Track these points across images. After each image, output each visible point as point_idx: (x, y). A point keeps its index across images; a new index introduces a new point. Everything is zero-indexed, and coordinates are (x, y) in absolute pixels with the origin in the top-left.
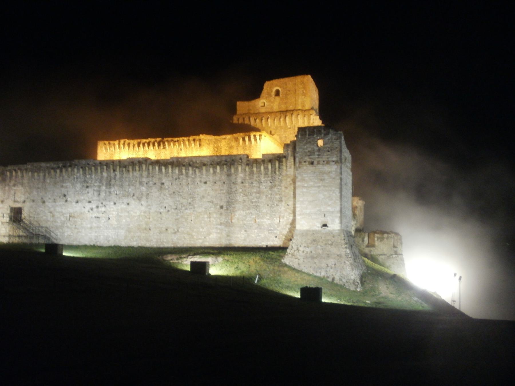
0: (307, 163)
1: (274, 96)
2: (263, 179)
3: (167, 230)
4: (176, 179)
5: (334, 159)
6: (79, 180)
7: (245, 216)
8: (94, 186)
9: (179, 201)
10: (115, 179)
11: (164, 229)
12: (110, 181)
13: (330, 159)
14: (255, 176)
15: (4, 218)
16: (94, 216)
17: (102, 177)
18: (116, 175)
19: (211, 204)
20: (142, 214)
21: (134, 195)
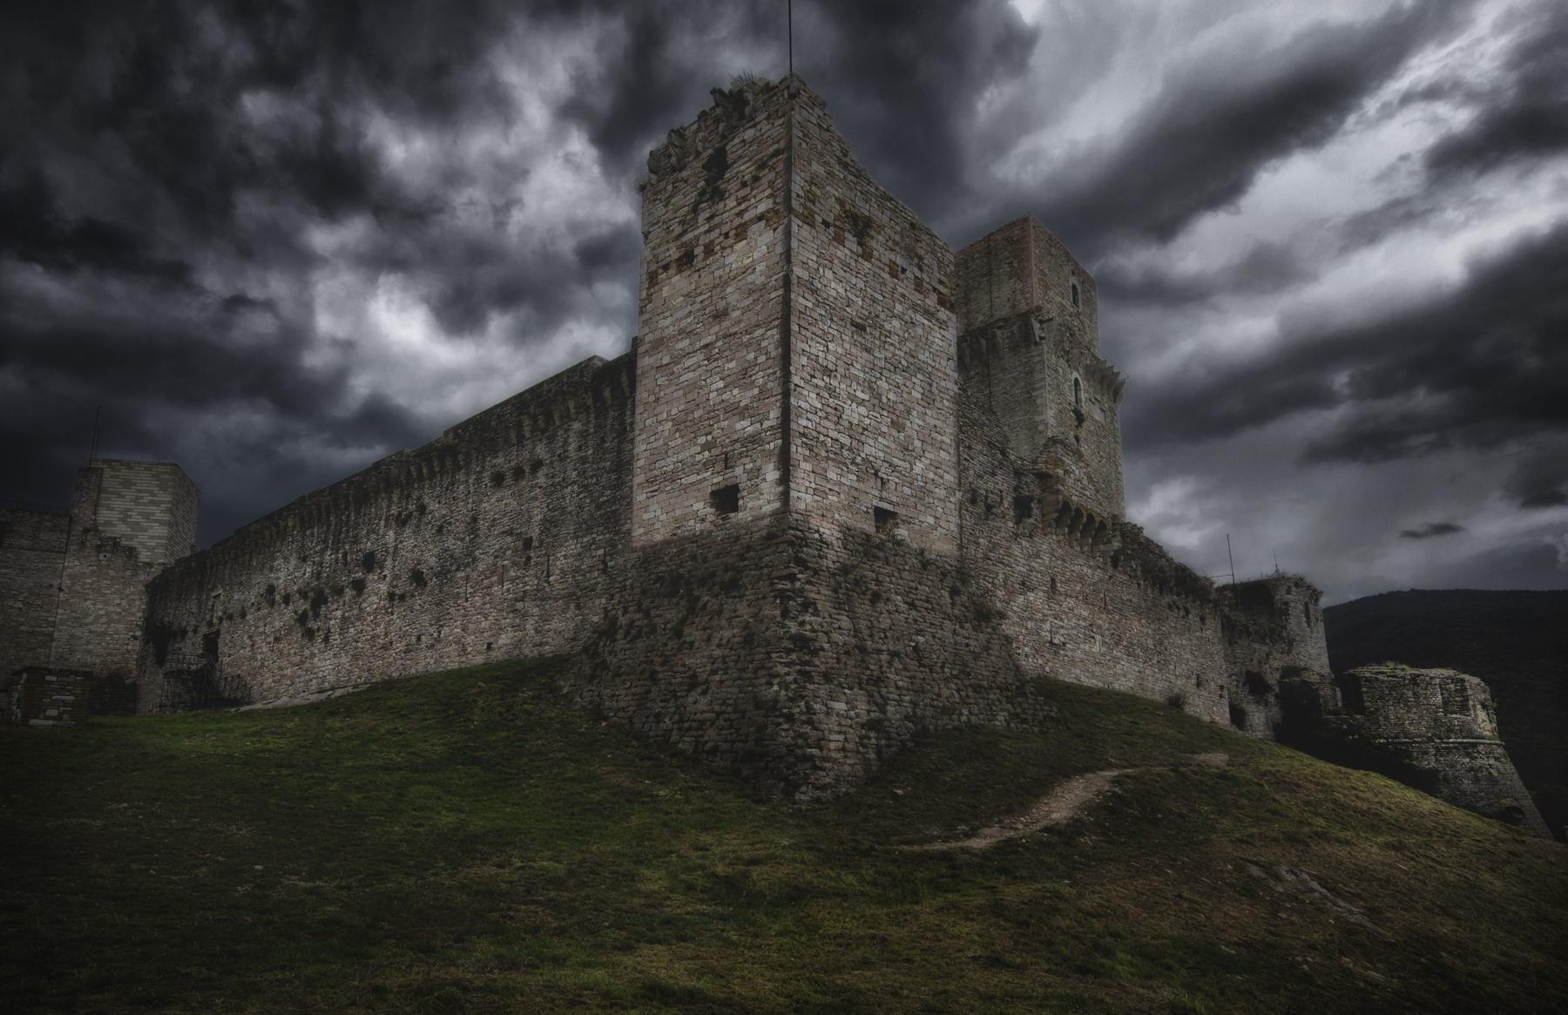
11: (414, 639)
19: (509, 539)
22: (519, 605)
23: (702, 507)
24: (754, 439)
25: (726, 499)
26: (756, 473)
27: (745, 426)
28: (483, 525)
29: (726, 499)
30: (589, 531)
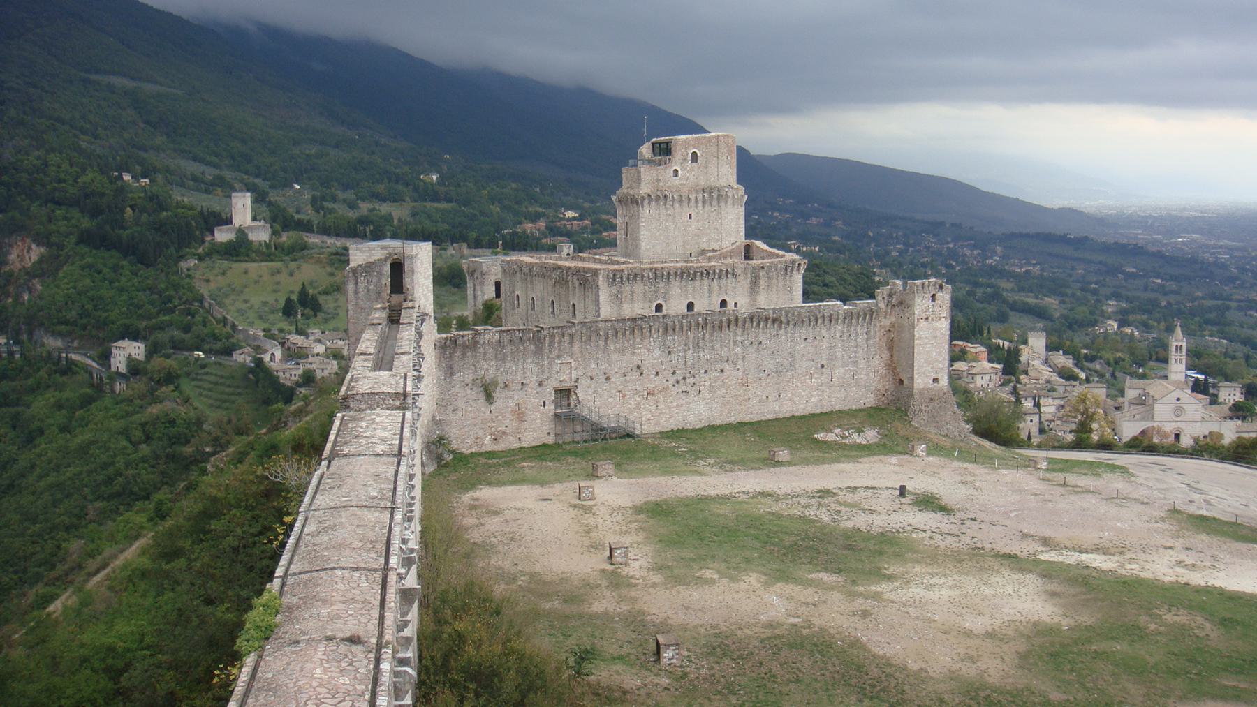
2: (859, 332)
6: (657, 344)
7: (844, 373)
10: (703, 339)
11: (764, 398)
12: (698, 343)
15: (546, 407)
16: (681, 390)
17: (688, 338)
18: (704, 335)
20: (740, 381)
23: (931, 382)
24: (942, 369)
25: (936, 380)
26: (943, 376)
27: (941, 366)
28: (798, 356)
29: (936, 380)
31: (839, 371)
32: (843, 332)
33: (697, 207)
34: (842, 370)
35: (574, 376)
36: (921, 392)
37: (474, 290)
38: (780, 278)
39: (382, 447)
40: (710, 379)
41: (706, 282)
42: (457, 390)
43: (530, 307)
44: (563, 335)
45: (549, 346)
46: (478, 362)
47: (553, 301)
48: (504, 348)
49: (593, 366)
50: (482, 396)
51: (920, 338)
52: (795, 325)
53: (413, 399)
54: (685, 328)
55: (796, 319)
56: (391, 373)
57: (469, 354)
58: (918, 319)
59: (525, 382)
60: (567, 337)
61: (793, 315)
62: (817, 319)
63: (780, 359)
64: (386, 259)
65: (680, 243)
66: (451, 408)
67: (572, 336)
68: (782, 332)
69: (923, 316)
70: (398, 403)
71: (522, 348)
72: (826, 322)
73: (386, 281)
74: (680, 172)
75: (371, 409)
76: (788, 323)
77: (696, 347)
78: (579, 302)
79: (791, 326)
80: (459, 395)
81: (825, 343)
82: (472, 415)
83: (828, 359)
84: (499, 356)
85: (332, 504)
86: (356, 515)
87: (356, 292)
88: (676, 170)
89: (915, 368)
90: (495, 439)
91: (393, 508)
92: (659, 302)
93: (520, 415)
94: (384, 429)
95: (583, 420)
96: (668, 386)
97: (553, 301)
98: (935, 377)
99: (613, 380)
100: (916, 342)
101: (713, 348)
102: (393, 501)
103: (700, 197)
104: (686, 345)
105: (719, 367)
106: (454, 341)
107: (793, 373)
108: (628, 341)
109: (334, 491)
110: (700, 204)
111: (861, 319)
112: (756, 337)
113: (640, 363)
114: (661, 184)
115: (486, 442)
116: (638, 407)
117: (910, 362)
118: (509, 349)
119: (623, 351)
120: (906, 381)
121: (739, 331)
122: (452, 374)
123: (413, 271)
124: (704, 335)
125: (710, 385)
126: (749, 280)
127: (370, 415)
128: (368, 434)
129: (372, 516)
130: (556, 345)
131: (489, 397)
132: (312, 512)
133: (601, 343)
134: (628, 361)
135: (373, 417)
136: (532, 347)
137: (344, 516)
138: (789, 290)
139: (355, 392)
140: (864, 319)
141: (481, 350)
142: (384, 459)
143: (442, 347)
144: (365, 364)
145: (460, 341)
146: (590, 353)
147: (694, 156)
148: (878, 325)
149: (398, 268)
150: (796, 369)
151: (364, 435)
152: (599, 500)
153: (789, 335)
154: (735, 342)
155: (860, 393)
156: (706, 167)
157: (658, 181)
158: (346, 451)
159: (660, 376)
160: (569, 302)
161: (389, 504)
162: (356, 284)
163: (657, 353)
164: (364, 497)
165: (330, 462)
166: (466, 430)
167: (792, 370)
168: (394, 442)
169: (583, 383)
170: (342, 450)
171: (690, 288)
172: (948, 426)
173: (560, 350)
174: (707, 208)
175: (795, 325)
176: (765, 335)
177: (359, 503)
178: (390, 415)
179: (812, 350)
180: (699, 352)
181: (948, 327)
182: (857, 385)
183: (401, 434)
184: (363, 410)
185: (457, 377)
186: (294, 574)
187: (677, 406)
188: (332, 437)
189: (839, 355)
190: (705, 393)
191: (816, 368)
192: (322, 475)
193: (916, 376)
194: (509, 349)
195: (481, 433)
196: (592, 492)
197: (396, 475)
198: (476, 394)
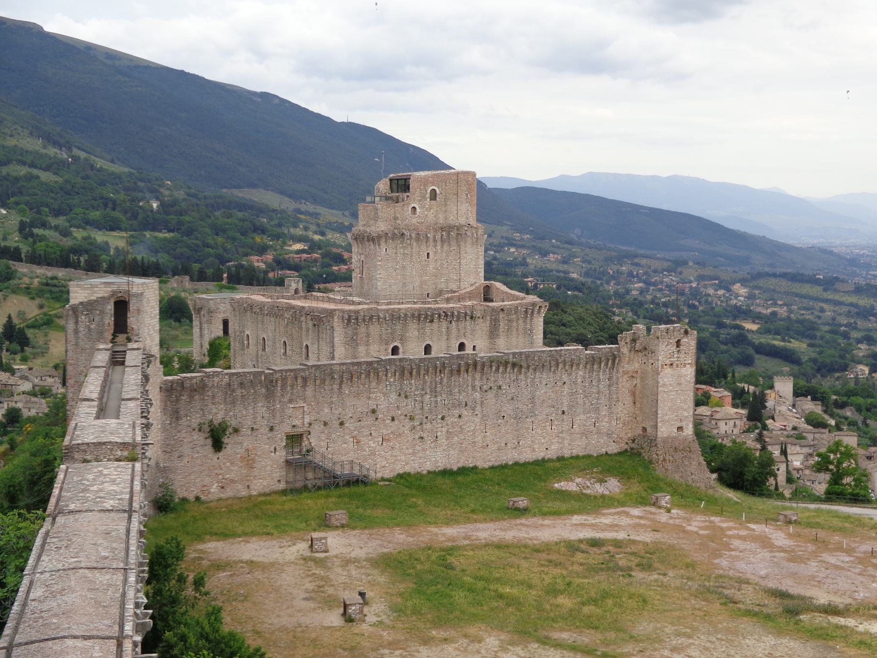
0: (668, 366)
1: (428, 200)
2: (601, 377)
3: (506, 444)
4: (514, 381)
5: (690, 362)
8: (415, 395)
9: (518, 408)
11: (503, 445)
12: (436, 387)
13: (686, 362)
14: (595, 373)
15: (277, 453)
16: (417, 437)
17: (425, 382)
18: (442, 379)
19: (552, 409)
21: (466, 405)
22: (561, 435)
23: (675, 430)
24: (687, 417)
25: (680, 429)
27: (686, 414)
29: (680, 429)
30: (589, 412)
31: (580, 418)
32: (584, 377)
33: (435, 246)
34: (582, 417)
35: (307, 420)
36: (665, 440)
37: (201, 328)
38: (521, 321)
39: (111, 502)
40: (447, 425)
41: (444, 324)
42: (184, 435)
43: (260, 347)
44: (296, 378)
45: (281, 389)
46: (206, 405)
47: (285, 342)
48: (233, 391)
49: (326, 410)
50: (209, 442)
51: (664, 385)
52: (535, 370)
53: (143, 449)
54: (422, 372)
55: (537, 364)
56: (117, 421)
57: (197, 397)
58: (662, 366)
59: (255, 427)
60: (299, 380)
61: (534, 359)
62: (557, 365)
63: (520, 406)
64: (109, 298)
65: (417, 284)
66: (177, 454)
67: (305, 380)
68: (522, 377)
69: (668, 362)
70: (126, 453)
71: (252, 391)
72: (567, 367)
73: (109, 320)
74: (418, 210)
75: (97, 460)
76: (528, 367)
77: (435, 393)
78: (313, 344)
79: (531, 370)
80: (185, 440)
81: (566, 389)
82: (199, 461)
83: (569, 406)
84: (228, 399)
85: (60, 566)
86: (86, 577)
87: (76, 331)
88: (414, 208)
89: (659, 416)
90: (223, 488)
91: (125, 569)
92: (396, 344)
93: (249, 461)
94: (113, 482)
95: (316, 467)
96: (404, 432)
97: (285, 342)
98: (679, 425)
99: (347, 425)
100: (660, 389)
101: (451, 393)
102: (127, 564)
103: (438, 237)
104: (423, 390)
105: (456, 412)
106: (181, 383)
107: (533, 419)
108: (364, 385)
109: (62, 551)
110: (439, 243)
111: (603, 364)
112: (495, 381)
113: (375, 407)
114: (399, 222)
115: (212, 490)
116: (373, 453)
117: (654, 410)
118: (239, 392)
119: (358, 395)
120: (649, 430)
121: (478, 376)
122: (178, 419)
123: (139, 311)
124: (442, 379)
125: (448, 431)
126: (488, 322)
127: (97, 467)
128: (95, 488)
129: (103, 578)
130: (289, 388)
131: (218, 445)
132: (38, 575)
133: (336, 387)
134: (362, 405)
135: (100, 469)
136: (264, 391)
137: (73, 580)
138: (529, 333)
139: (80, 442)
140: (607, 364)
141: (210, 393)
142: (112, 514)
143: (167, 391)
144: (88, 410)
145: (187, 384)
146: (323, 397)
147: (434, 195)
148: (621, 370)
149: (121, 307)
150: (535, 415)
151: (92, 488)
152: (333, 552)
153: (529, 380)
154: (473, 387)
155: (602, 441)
156: (446, 205)
157: (396, 218)
158: (72, 507)
159: (396, 422)
160: (301, 343)
161: (122, 565)
162: (77, 322)
163: (393, 396)
164: (94, 558)
165: (54, 519)
166: (192, 477)
167: (531, 417)
168: (123, 496)
169: (317, 428)
170: (67, 506)
171: (428, 330)
172: (693, 477)
173: (292, 394)
174: (446, 248)
175: (535, 370)
176: (504, 379)
177: (89, 565)
178: (118, 467)
179: (553, 396)
180: (436, 396)
181: (693, 374)
182: (599, 433)
183: (132, 488)
184: (89, 461)
185: (183, 422)
186: (20, 645)
187: (414, 454)
188: (56, 492)
189: (580, 401)
190: (443, 440)
191: (557, 414)
192: (47, 534)
193: (660, 425)
194: (239, 392)
195: (207, 480)
196: (326, 544)
197: (128, 531)
198: (202, 440)
